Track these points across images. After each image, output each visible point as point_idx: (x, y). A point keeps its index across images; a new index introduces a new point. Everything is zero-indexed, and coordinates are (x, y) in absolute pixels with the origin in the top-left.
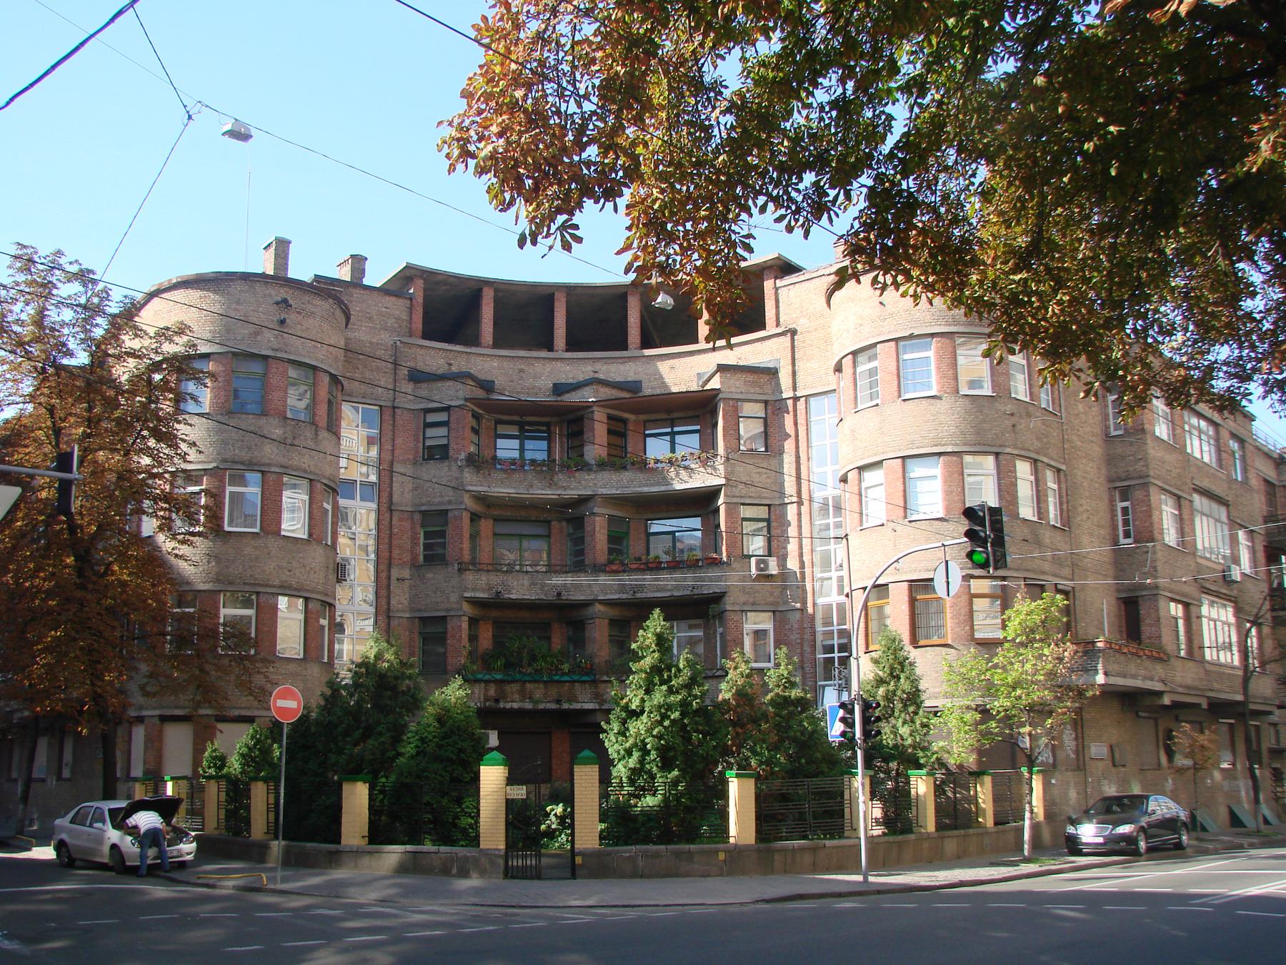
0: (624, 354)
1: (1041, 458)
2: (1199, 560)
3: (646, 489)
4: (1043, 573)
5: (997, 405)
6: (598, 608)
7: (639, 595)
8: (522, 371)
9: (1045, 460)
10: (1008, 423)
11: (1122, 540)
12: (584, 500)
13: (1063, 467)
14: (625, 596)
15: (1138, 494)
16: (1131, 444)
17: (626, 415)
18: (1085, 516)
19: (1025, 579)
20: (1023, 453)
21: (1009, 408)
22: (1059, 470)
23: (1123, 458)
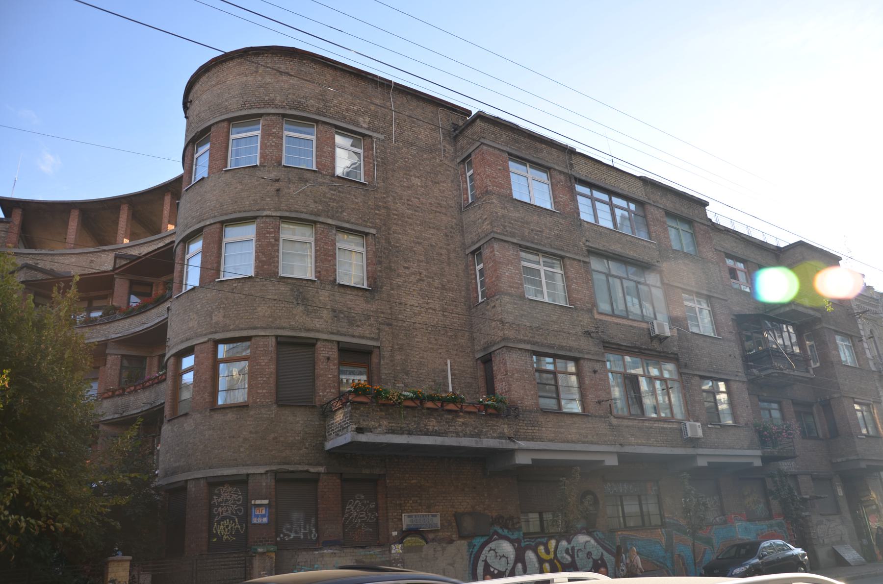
0: (157, 236)
1: (321, 219)
2: (597, 316)
3: (137, 329)
4: (308, 330)
5: (259, 174)
6: (102, 427)
7: (125, 414)
8: (92, 262)
9: (330, 221)
10: (271, 189)
11: (480, 300)
12: (104, 344)
13: (373, 231)
14: (116, 416)
15: (486, 252)
16: (480, 208)
17: (149, 279)
18: (413, 278)
19: (277, 337)
20: (287, 214)
21: (273, 175)
22: (367, 234)
23: (474, 222)
